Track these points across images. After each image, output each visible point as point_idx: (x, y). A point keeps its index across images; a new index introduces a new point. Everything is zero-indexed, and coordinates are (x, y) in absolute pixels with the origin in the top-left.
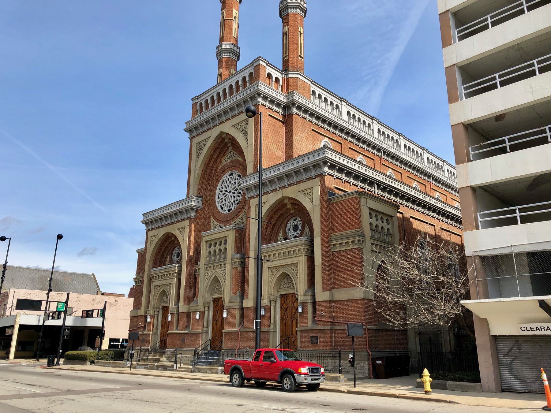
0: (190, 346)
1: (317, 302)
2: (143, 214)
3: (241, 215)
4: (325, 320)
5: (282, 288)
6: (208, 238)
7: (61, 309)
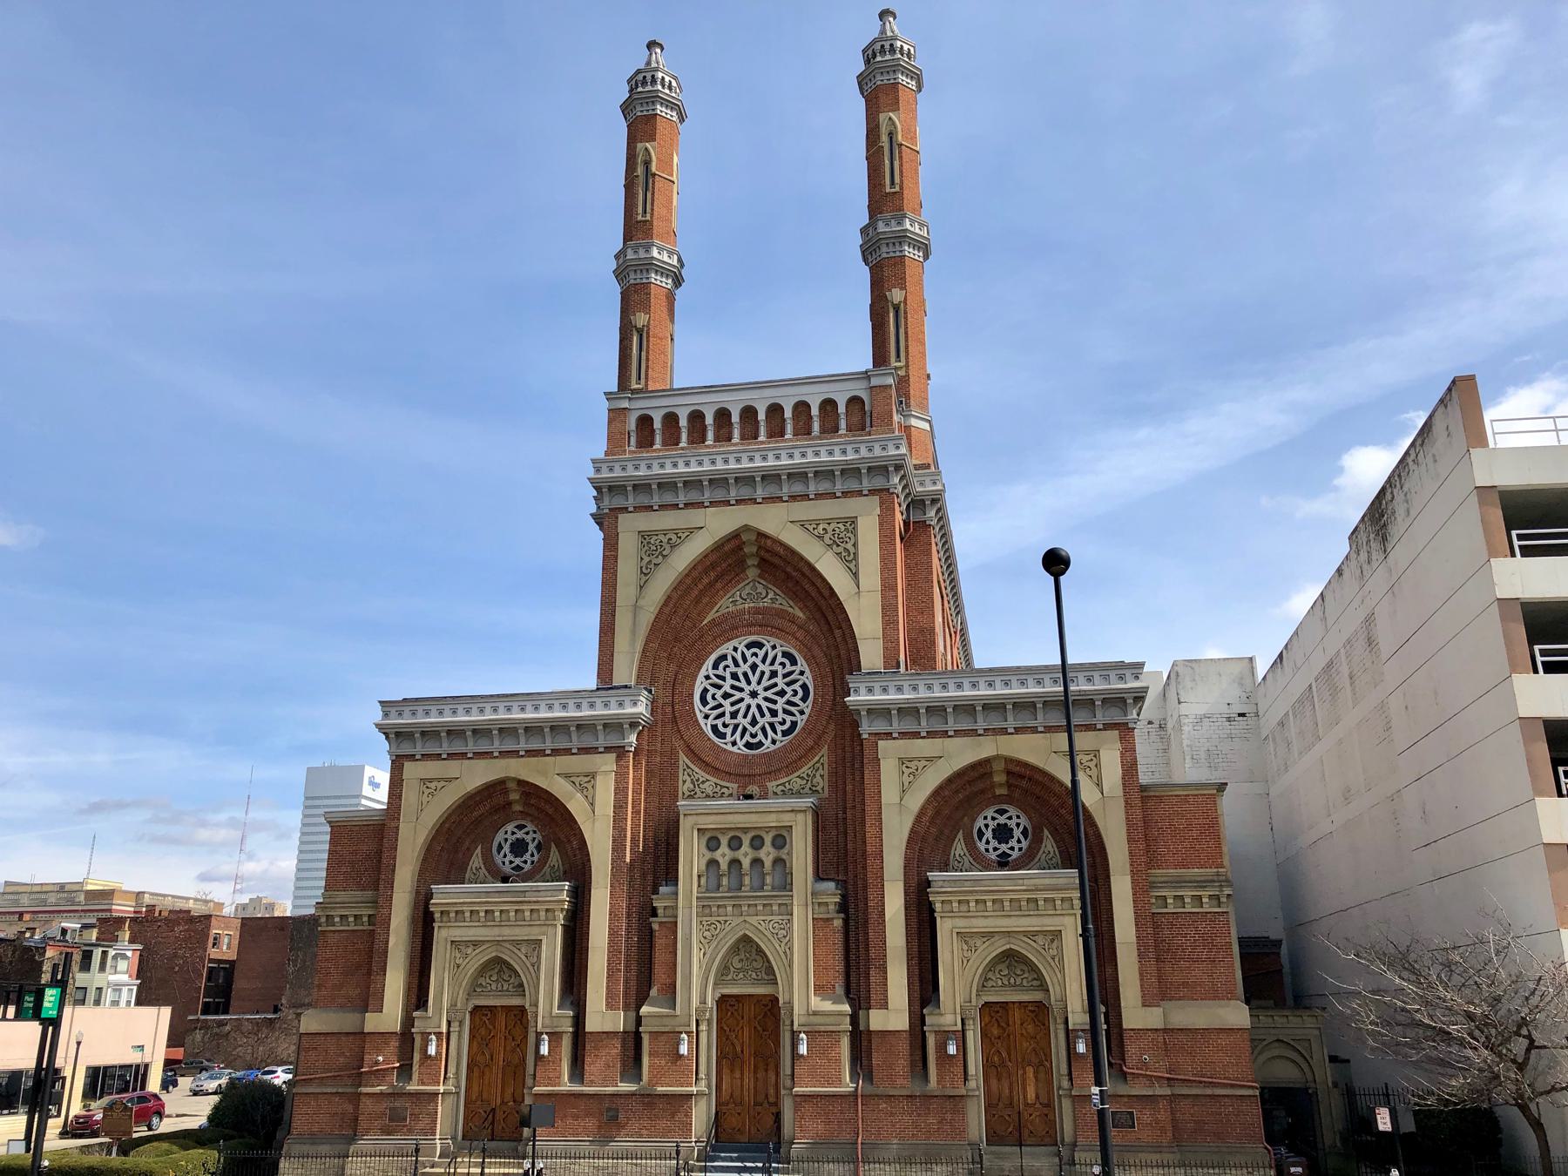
0: (644, 1132)
1: (1126, 1030)
2: (380, 702)
3: (806, 767)
4: (1155, 1074)
5: (993, 986)
6: (710, 822)
7: (51, 1012)
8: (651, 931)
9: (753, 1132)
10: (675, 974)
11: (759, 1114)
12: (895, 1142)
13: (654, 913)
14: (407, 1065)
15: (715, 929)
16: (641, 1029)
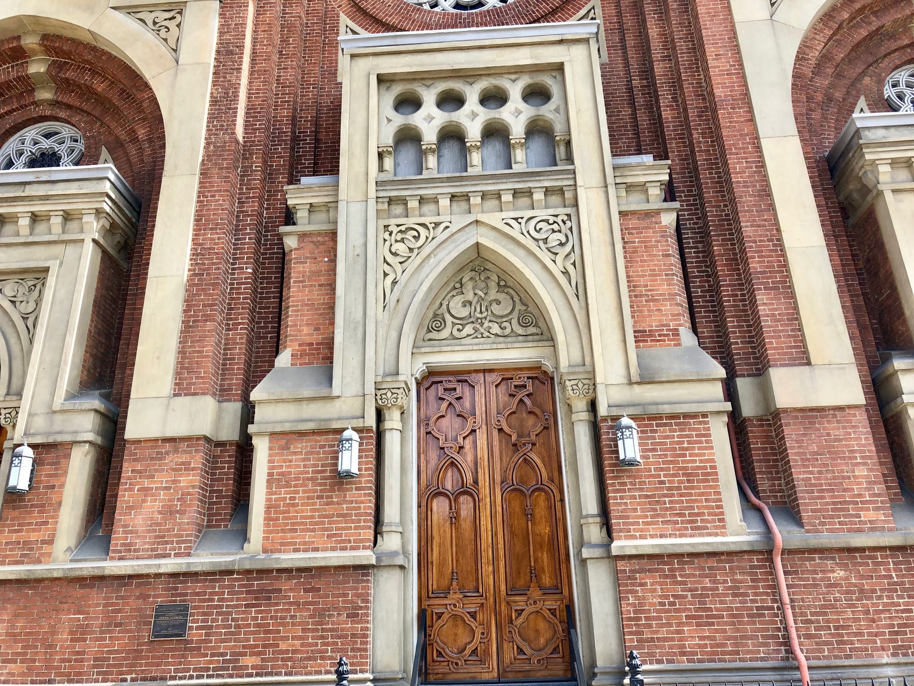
0: (249, 661)
8: (283, 256)
9: (507, 661)
10: (332, 323)
11: (520, 612)
12: (885, 660)
13: (289, 217)
15: (417, 238)
16: (251, 429)
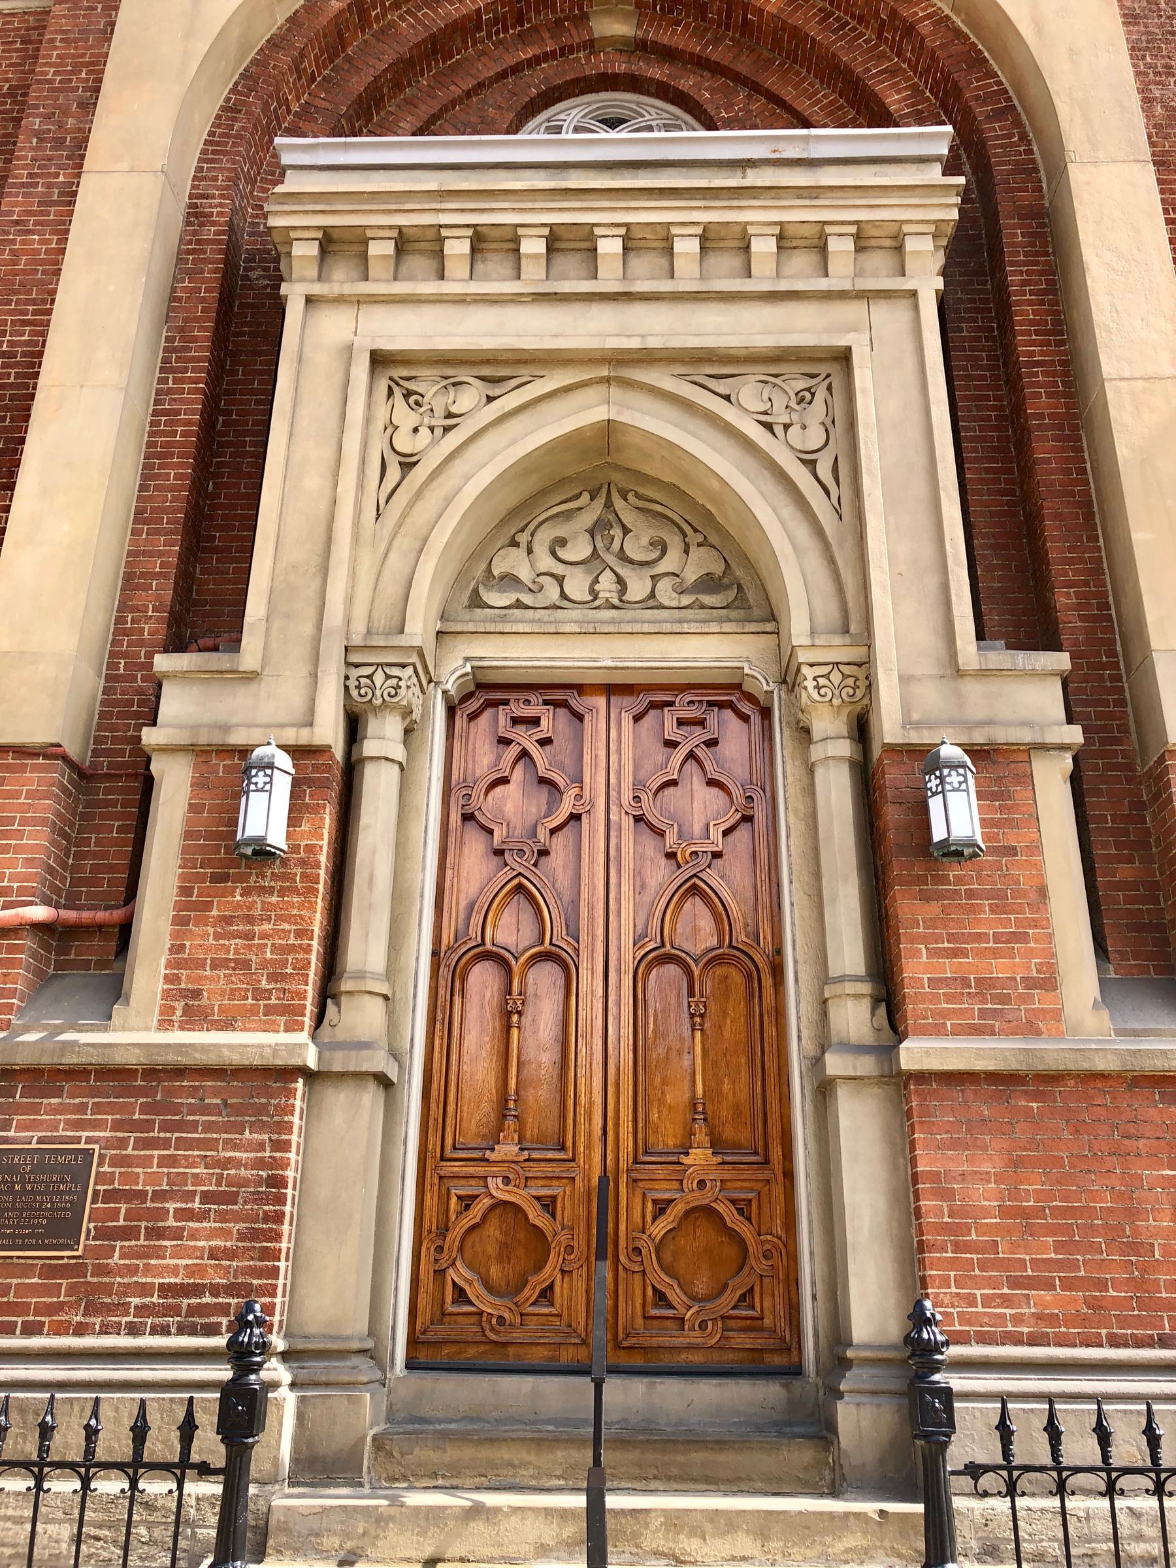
14: (98, 928)
